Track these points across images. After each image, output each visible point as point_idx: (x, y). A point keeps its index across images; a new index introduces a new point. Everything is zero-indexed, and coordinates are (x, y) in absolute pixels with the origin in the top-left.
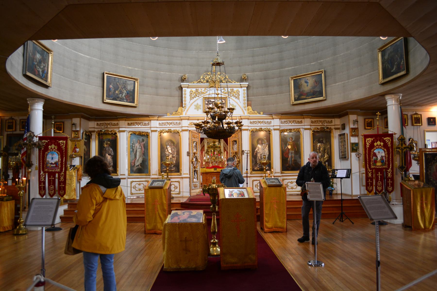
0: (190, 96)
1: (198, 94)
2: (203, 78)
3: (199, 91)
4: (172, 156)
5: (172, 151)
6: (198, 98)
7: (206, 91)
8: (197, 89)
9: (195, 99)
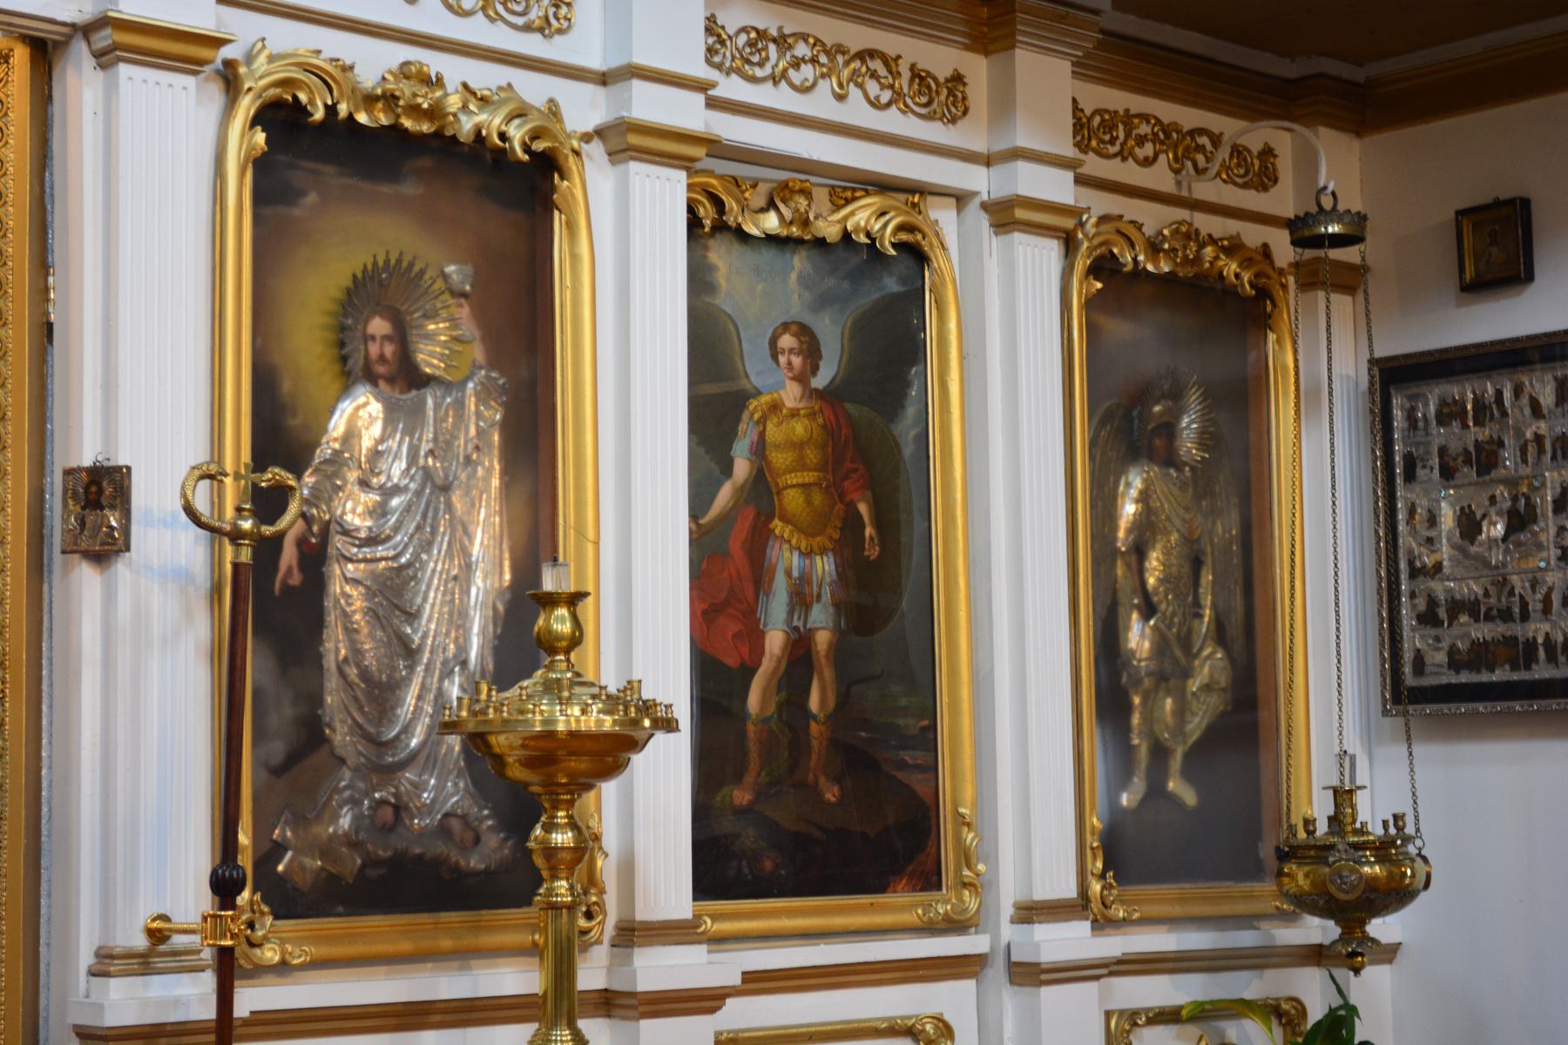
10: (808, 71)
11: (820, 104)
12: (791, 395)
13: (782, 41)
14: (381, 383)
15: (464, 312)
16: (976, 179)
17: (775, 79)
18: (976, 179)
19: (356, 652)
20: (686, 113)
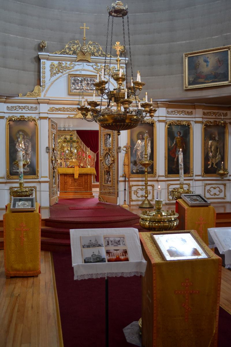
0: (51, 71)
1: (62, 69)
2: (68, 48)
3: (63, 65)
4: (26, 153)
5: (25, 146)
6: (62, 74)
7: (73, 65)
8: (61, 62)
9: (57, 76)
10: (177, 113)
11: (178, 115)
12: (179, 137)
13: (174, 111)
14: (141, 140)
15: (148, 134)
16: (194, 119)
17: (174, 114)
18: (194, 119)
19: (139, 157)
20: (164, 119)
